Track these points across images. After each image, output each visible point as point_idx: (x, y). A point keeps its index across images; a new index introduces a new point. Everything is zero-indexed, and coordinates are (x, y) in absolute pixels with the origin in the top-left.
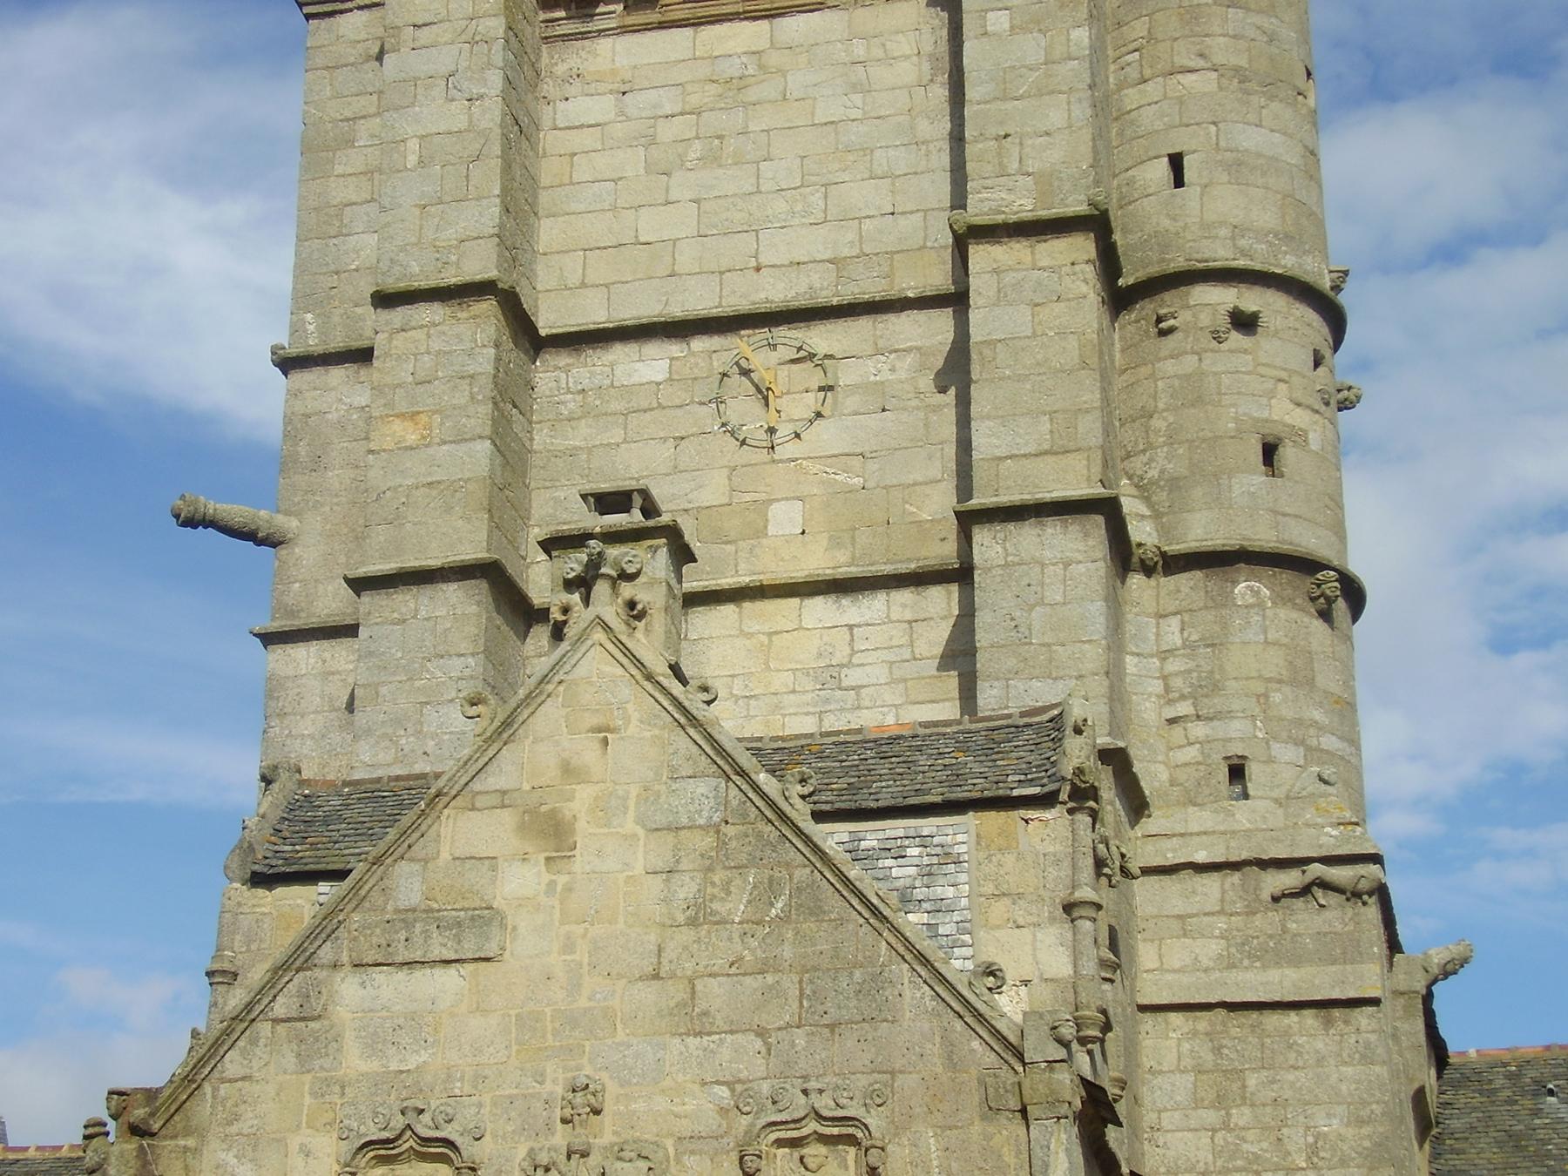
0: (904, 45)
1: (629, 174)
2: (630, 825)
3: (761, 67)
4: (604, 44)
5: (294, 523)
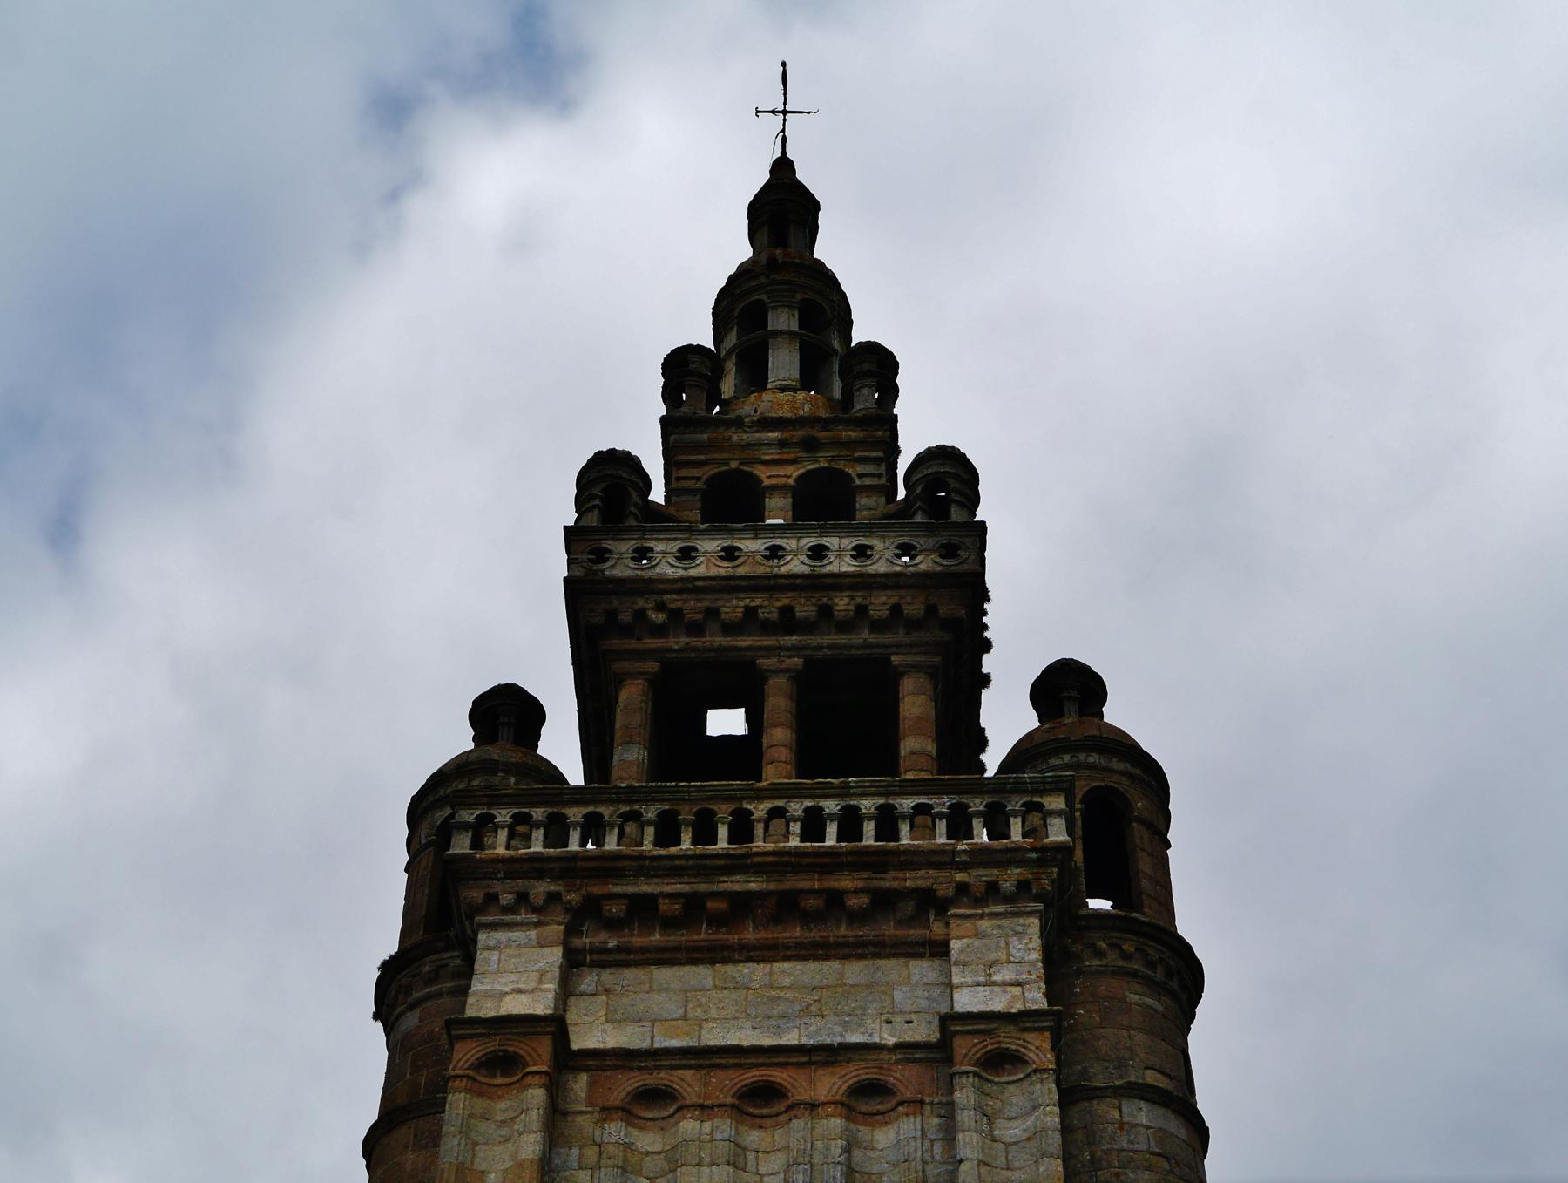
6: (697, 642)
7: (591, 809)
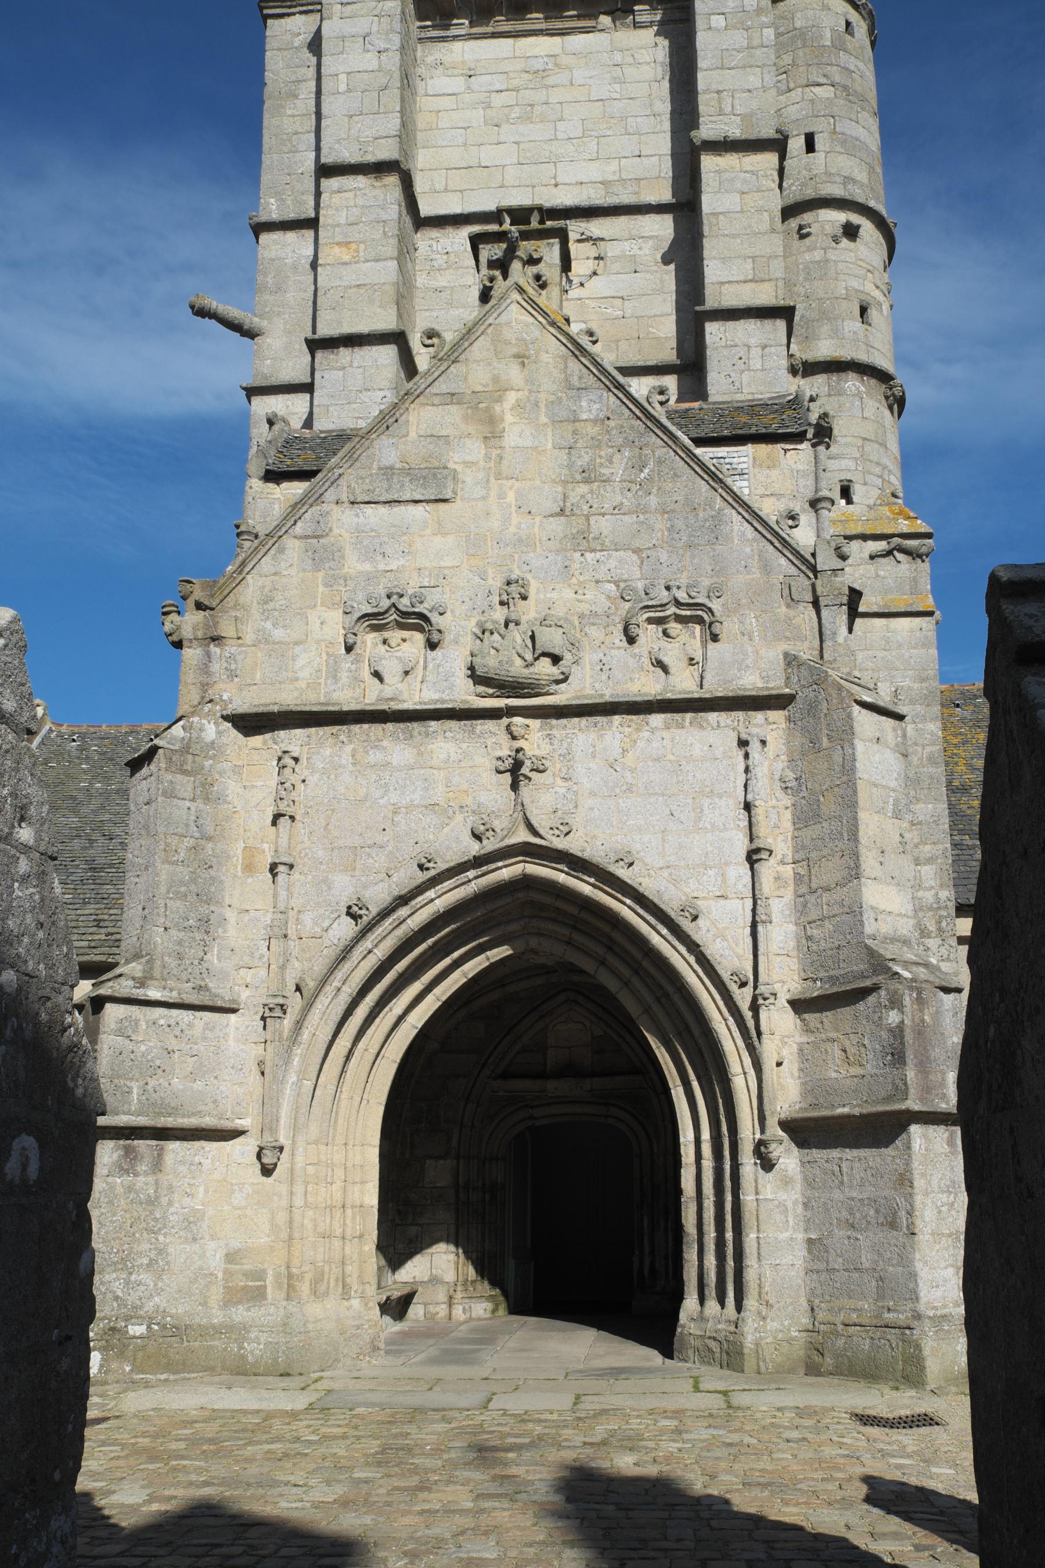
0: (645, 56)
2: (544, 419)
3: (556, 65)
4: (457, 46)
5: (265, 323)
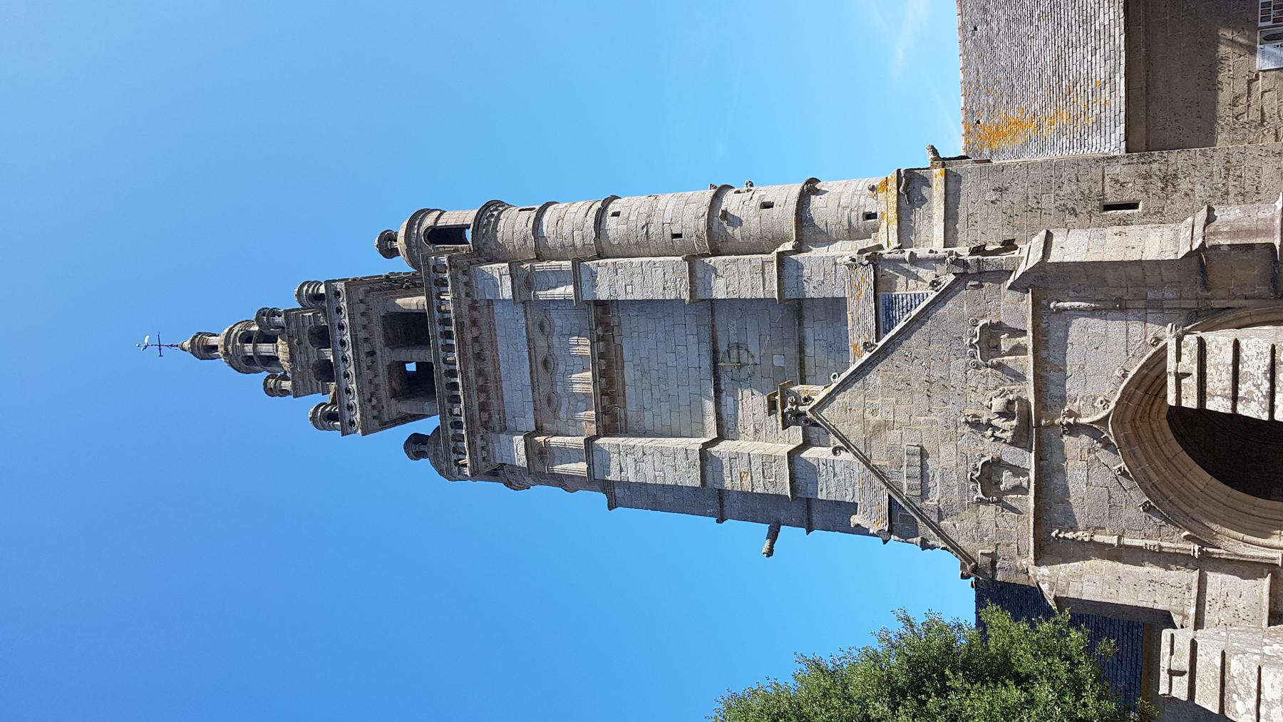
1: (668, 407)
6: (382, 387)
7: (449, 426)
